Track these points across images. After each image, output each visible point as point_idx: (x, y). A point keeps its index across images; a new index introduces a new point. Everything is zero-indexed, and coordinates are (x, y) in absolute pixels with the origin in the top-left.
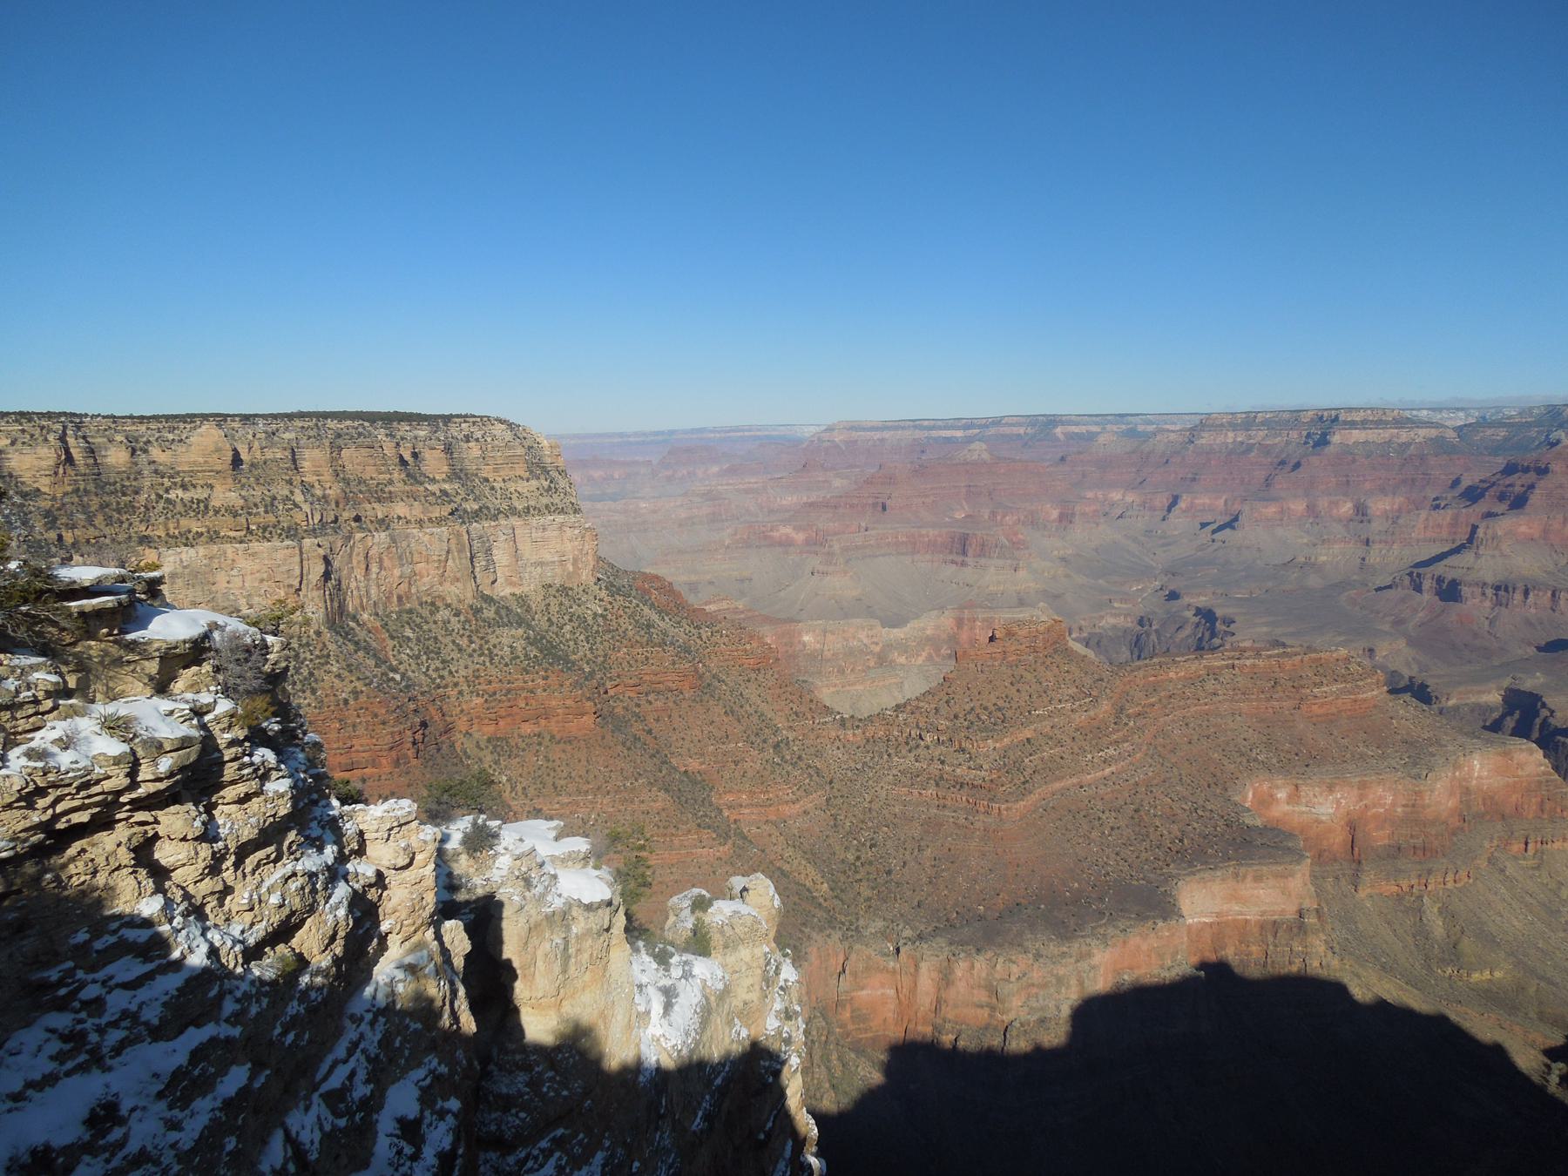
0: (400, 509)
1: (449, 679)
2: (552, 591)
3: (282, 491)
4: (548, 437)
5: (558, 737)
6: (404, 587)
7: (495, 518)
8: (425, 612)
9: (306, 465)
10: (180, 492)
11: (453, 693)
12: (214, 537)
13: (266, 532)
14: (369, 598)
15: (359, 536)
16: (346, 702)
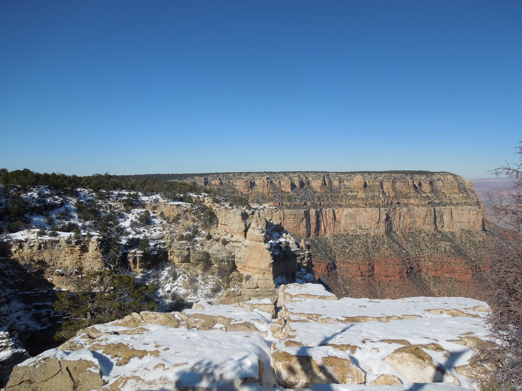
0: (412, 201)
1: (422, 255)
2: (464, 232)
3: (377, 194)
4: (468, 180)
5: (458, 280)
6: (411, 225)
7: (445, 206)
8: (417, 234)
9: (385, 187)
10: (350, 193)
11: (423, 260)
12: (357, 206)
13: (371, 206)
14: (399, 227)
15: (398, 208)
16: (388, 257)
